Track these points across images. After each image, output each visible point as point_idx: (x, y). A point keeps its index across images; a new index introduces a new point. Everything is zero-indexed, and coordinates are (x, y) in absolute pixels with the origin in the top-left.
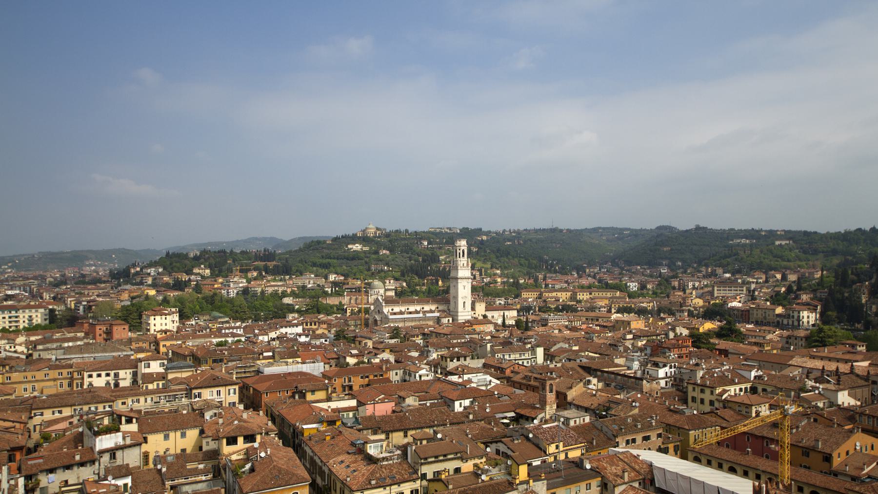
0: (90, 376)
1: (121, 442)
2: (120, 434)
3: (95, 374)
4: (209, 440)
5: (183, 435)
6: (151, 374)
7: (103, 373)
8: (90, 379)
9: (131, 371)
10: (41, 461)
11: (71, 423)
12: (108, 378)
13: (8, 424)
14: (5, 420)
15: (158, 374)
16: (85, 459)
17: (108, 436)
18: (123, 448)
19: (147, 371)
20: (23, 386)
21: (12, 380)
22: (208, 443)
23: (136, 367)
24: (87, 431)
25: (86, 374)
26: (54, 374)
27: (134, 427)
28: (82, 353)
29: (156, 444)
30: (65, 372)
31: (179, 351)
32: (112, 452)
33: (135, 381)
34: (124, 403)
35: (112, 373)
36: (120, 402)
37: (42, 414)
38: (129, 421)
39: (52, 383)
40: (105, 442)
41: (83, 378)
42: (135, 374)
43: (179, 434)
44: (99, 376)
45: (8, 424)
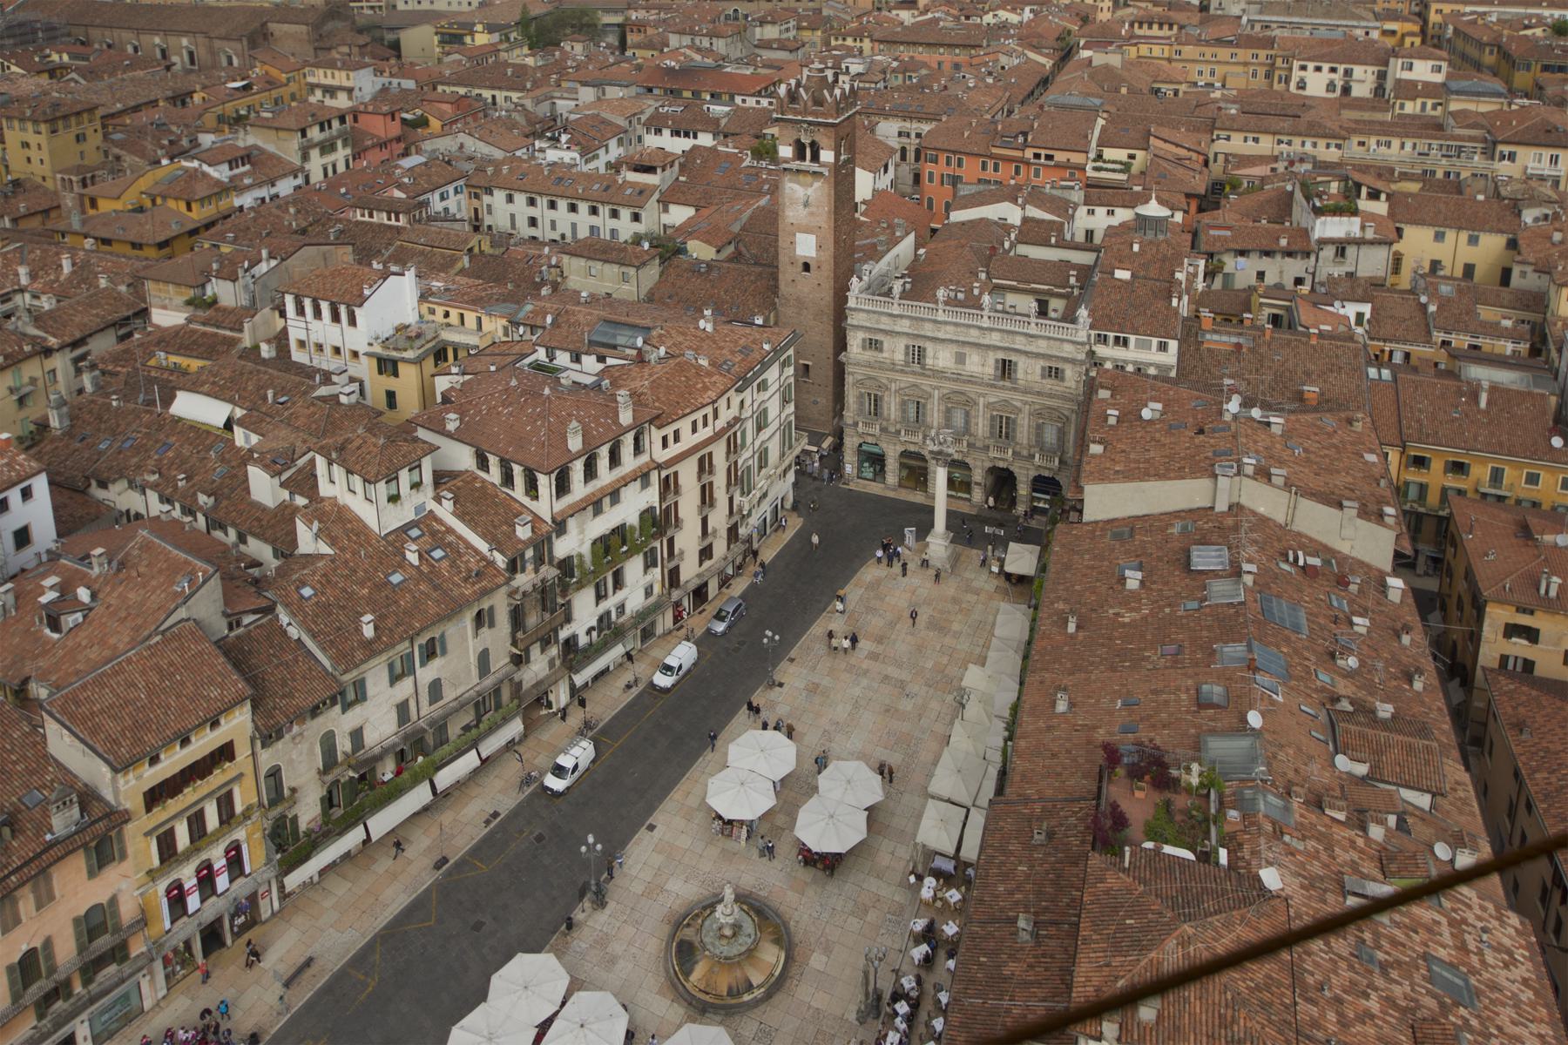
0: (1303, 68)
1: (1356, 231)
2: (1357, 220)
3: (1311, 66)
4: (1529, 269)
5: (1473, 241)
6: (1414, 83)
7: (1326, 67)
8: (1302, 73)
9: (1376, 69)
10: (1229, 233)
11: (1273, 170)
12: (1333, 76)
13: (1182, 152)
14: (1177, 145)
15: (1426, 84)
16: (1294, 248)
17: (1336, 219)
18: (1359, 242)
19: (1406, 75)
20: (1198, 67)
21: (1183, 56)
22: (1523, 274)
23: (1386, 64)
24: (1298, 196)
25: (1296, 64)
26: (1244, 54)
27: (1380, 207)
28: (1289, 15)
29: (1419, 243)
30: (1263, 54)
31: (1470, 31)
32: (1341, 246)
33: (1379, 90)
34: (1362, 144)
35: (1341, 68)
36: (1355, 140)
37: (1228, 139)
38: (1374, 195)
39: (1240, 69)
40: (1332, 227)
41: (1291, 69)
42: (1382, 76)
43: (1464, 236)
44: (1318, 69)
45: (1182, 152)
